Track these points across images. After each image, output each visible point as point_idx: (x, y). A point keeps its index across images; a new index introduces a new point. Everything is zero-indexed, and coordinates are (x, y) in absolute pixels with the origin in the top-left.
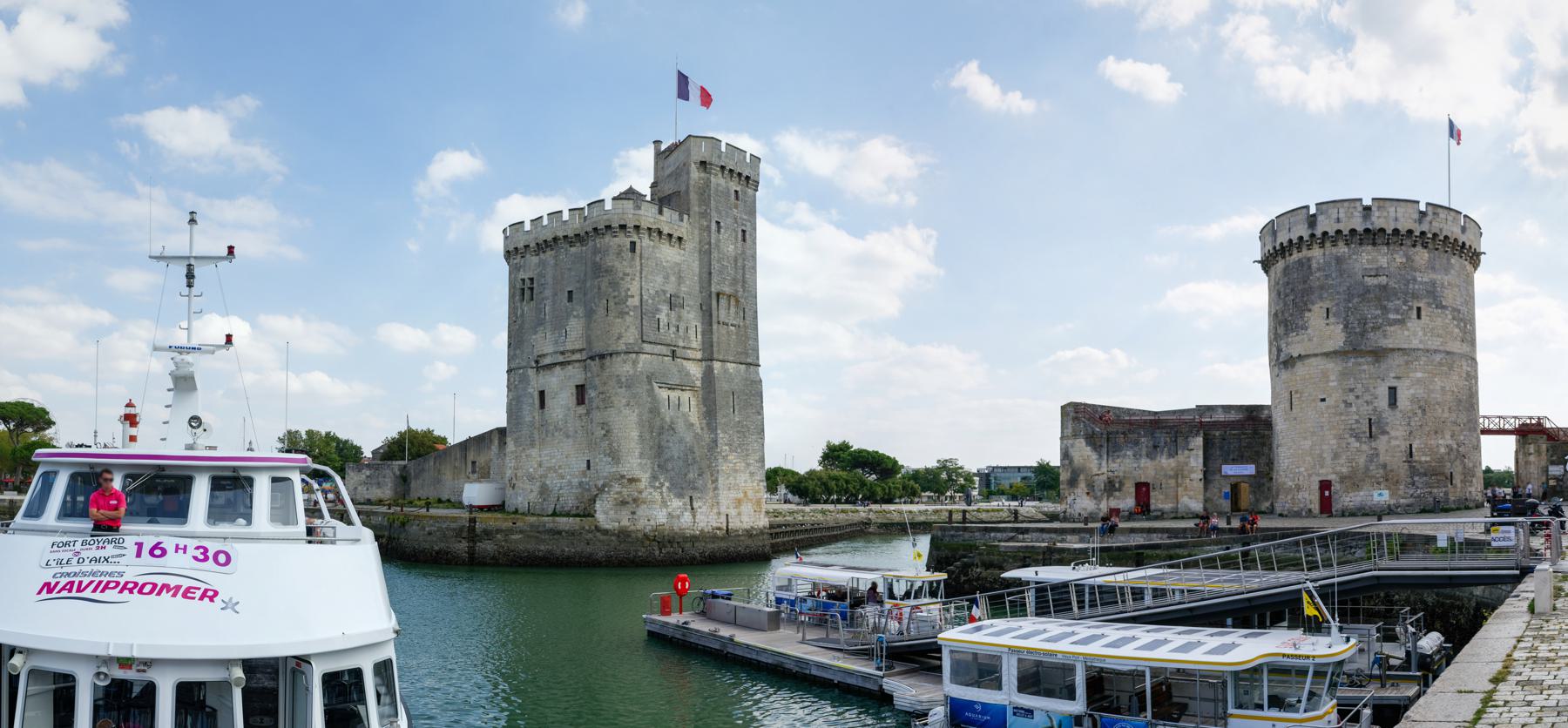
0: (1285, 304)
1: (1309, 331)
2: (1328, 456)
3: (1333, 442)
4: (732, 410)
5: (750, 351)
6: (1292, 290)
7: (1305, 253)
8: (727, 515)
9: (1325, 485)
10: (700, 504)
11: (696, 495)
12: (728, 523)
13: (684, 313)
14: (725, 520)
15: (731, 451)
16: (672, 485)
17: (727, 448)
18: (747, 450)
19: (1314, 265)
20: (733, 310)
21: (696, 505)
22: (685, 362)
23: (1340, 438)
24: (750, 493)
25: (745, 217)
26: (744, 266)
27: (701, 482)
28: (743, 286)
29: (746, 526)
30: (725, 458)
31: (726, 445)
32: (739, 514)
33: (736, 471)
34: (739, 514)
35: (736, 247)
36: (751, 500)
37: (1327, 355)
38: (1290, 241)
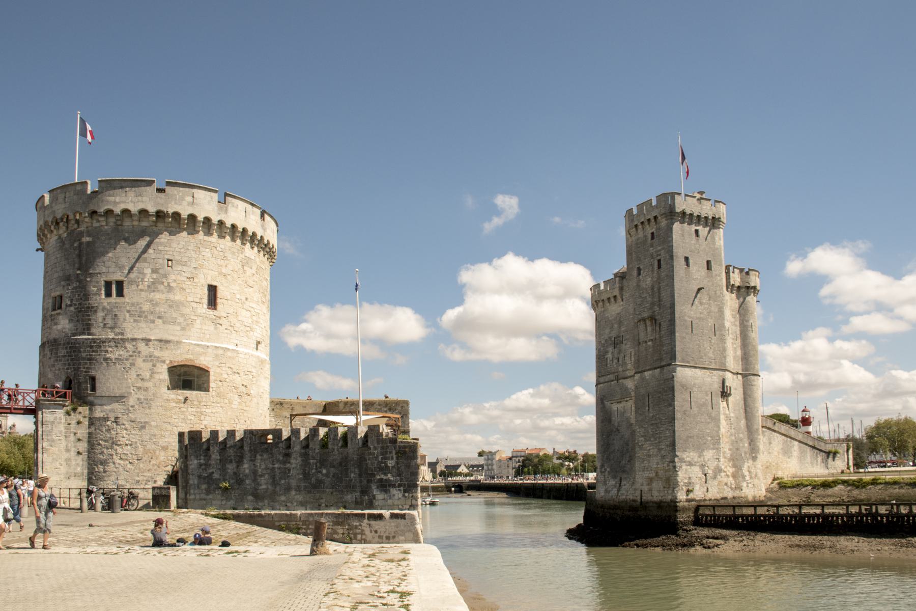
4: (647, 408)
5: (665, 356)
8: (641, 491)
10: (625, 483)
11: (624, 476)
12: (641, 496)
13: (623, 347)
14: (639, 495)
15: (646, 440)
16: (611, 469)
17: (643, 439)
18: (660, 438)
20: (649, 329)
21: (623, 483)
22: (624, 381)
24: (661, 473)
25: (659, 248)
26: (659, 289)
27: (629, 466)
28: (659, 306)
29: (655, 499)
30: (641, 447)
31: (642, 436)
32: (650, 490)
33: (649, 456)
34: (650, 490)
35: (652, 278)
36: (661, 478)
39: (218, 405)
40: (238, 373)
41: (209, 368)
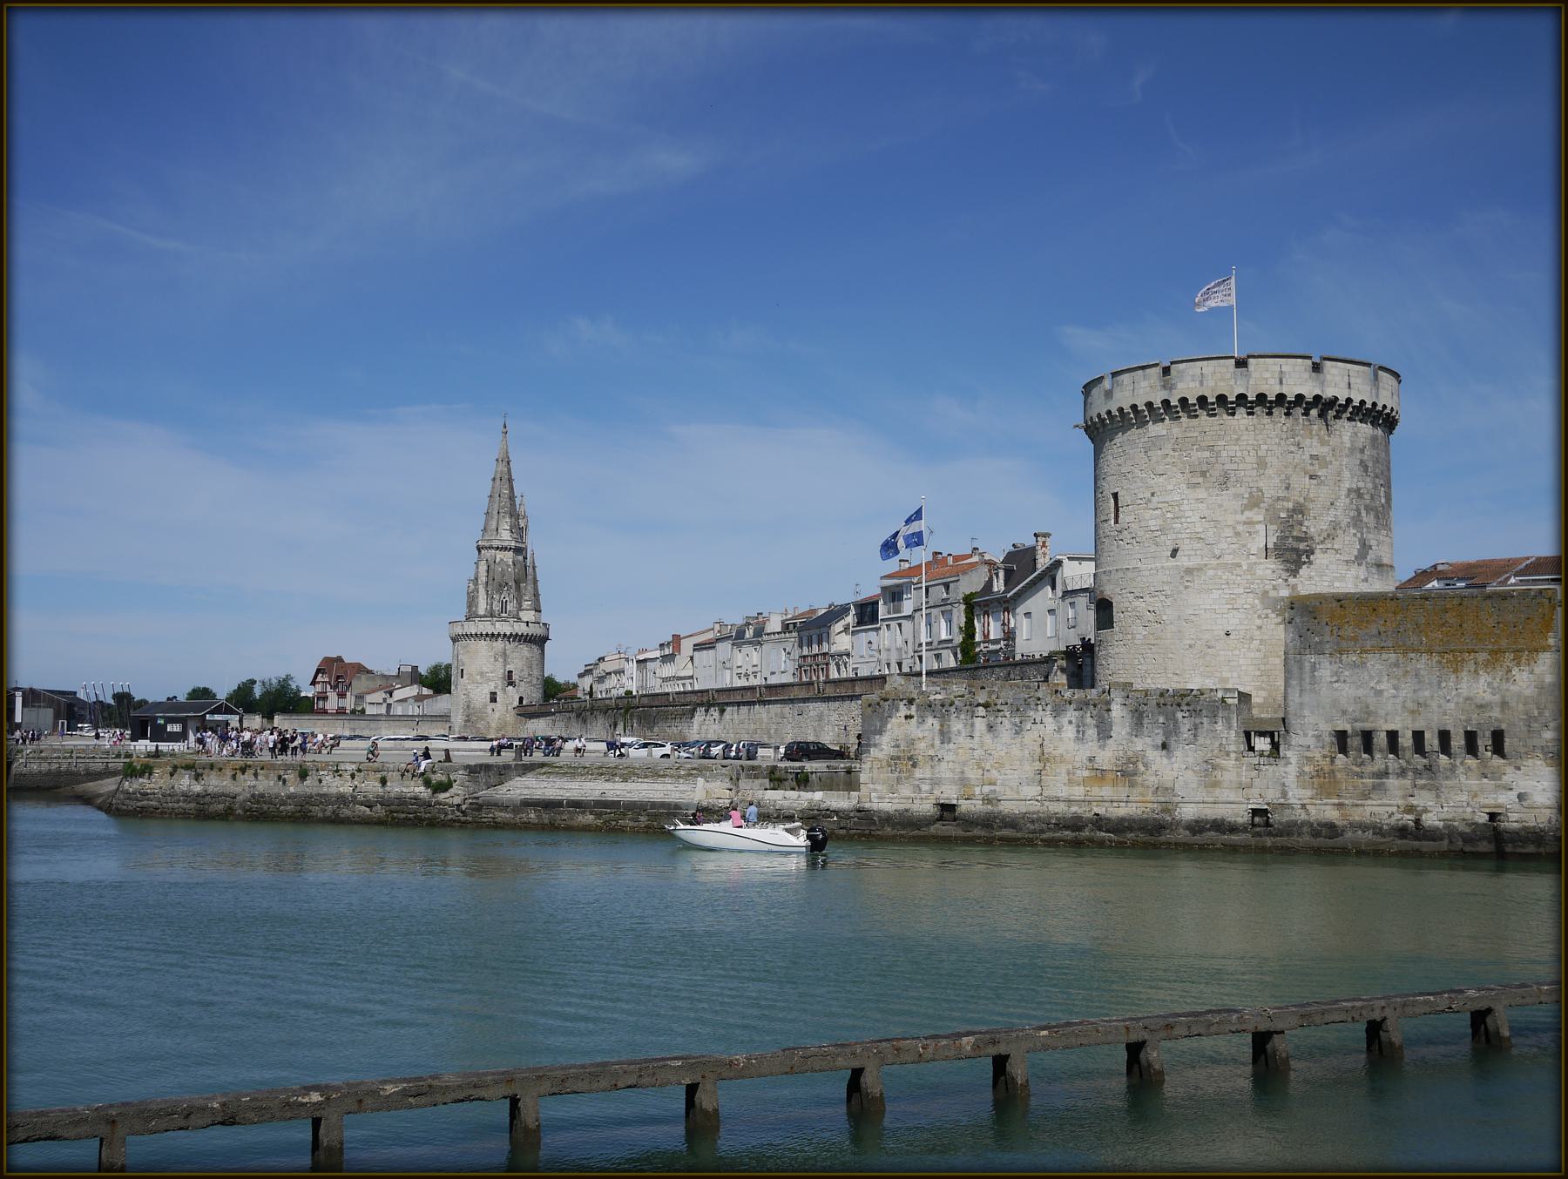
0: (1375, 487)
39: (1121, 643)
40: (1142, 598)
41: (1111, 598)
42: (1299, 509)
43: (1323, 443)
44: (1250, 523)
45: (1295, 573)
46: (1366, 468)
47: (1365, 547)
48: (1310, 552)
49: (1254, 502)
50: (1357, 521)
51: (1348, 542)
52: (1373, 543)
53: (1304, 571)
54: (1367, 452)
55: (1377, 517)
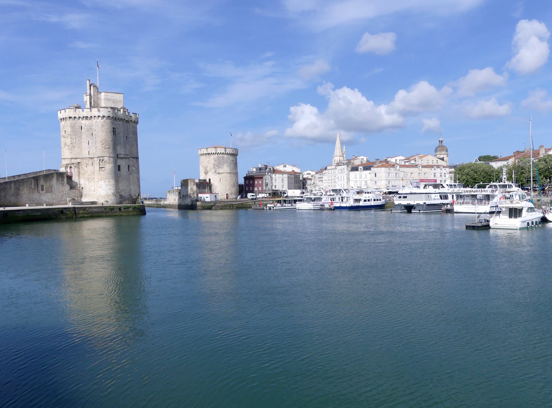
0: (218, 163)
1: (224, 169)
2: (228, 190)
3: (229, 187)
6: (220, 161)
7: (223, 155)
9: (227, 194)
19: (225, 158)
23: (229, 187)
37: (227, 173)
38: (223, 153)
42: (206, 167)
43: (209, 159)
44: (203, 169)
45: (206, 175)
46: (216, 161)
47: (216, 171)
48: (208, 172)
49: (203, 167)
50: (214, 168)
51: (213, 171)
52: (218, 170)
53: (207, 175)
54: (216, 159)
55: (218, 166)
